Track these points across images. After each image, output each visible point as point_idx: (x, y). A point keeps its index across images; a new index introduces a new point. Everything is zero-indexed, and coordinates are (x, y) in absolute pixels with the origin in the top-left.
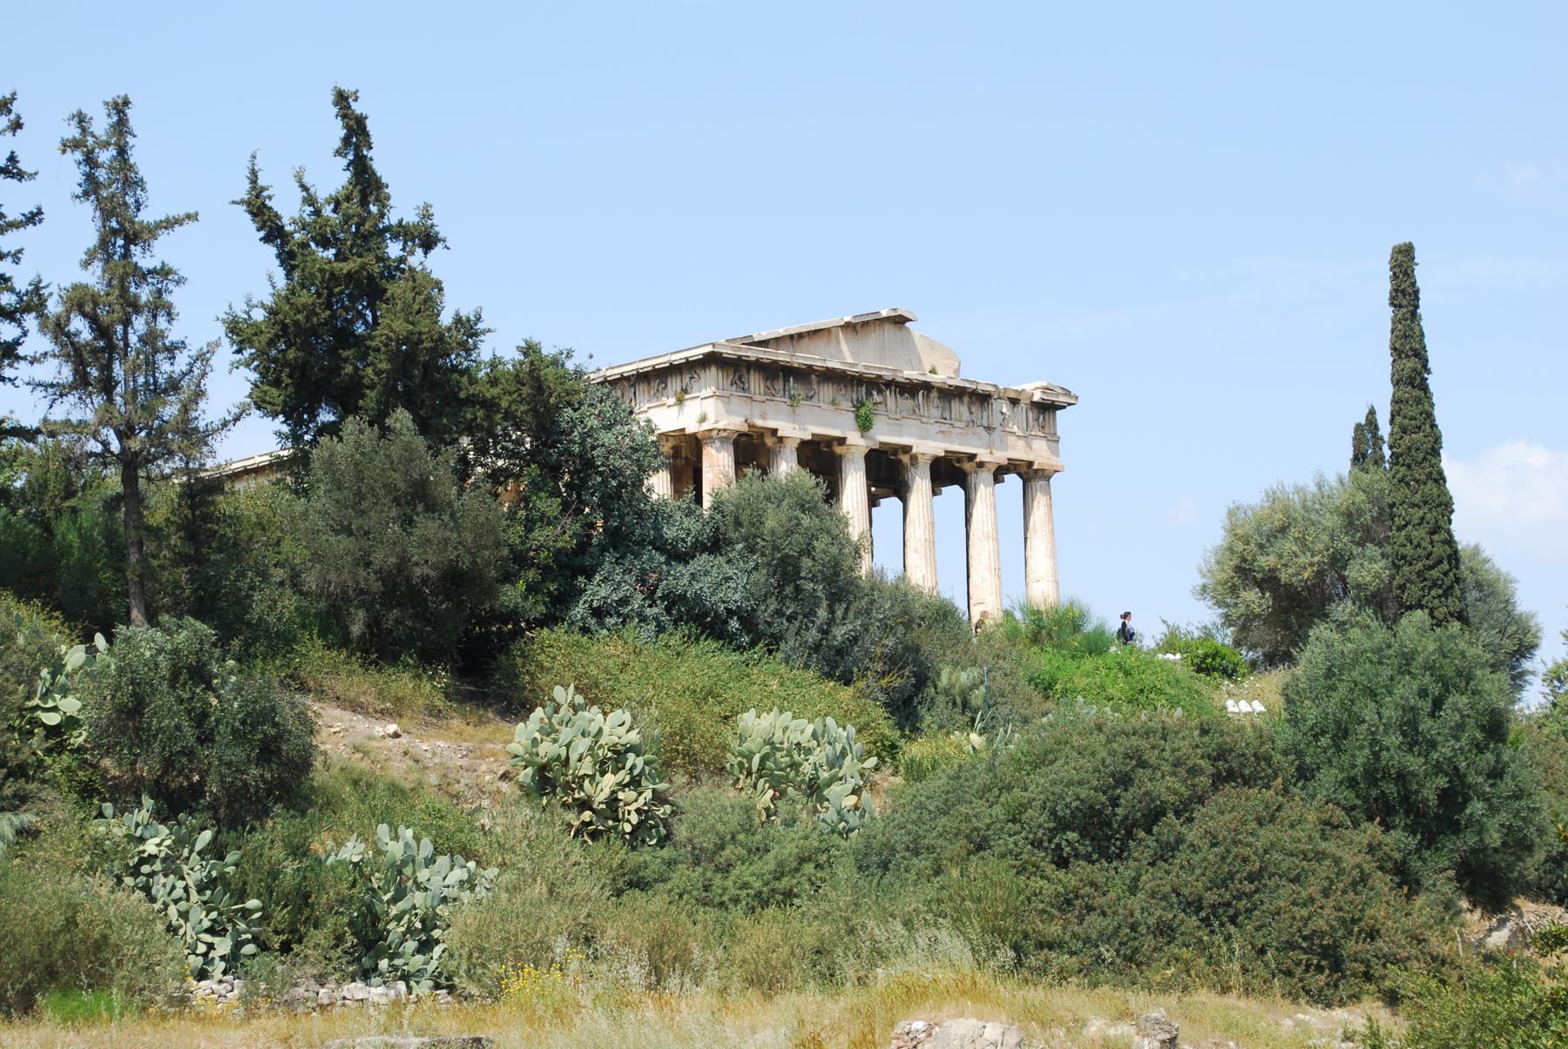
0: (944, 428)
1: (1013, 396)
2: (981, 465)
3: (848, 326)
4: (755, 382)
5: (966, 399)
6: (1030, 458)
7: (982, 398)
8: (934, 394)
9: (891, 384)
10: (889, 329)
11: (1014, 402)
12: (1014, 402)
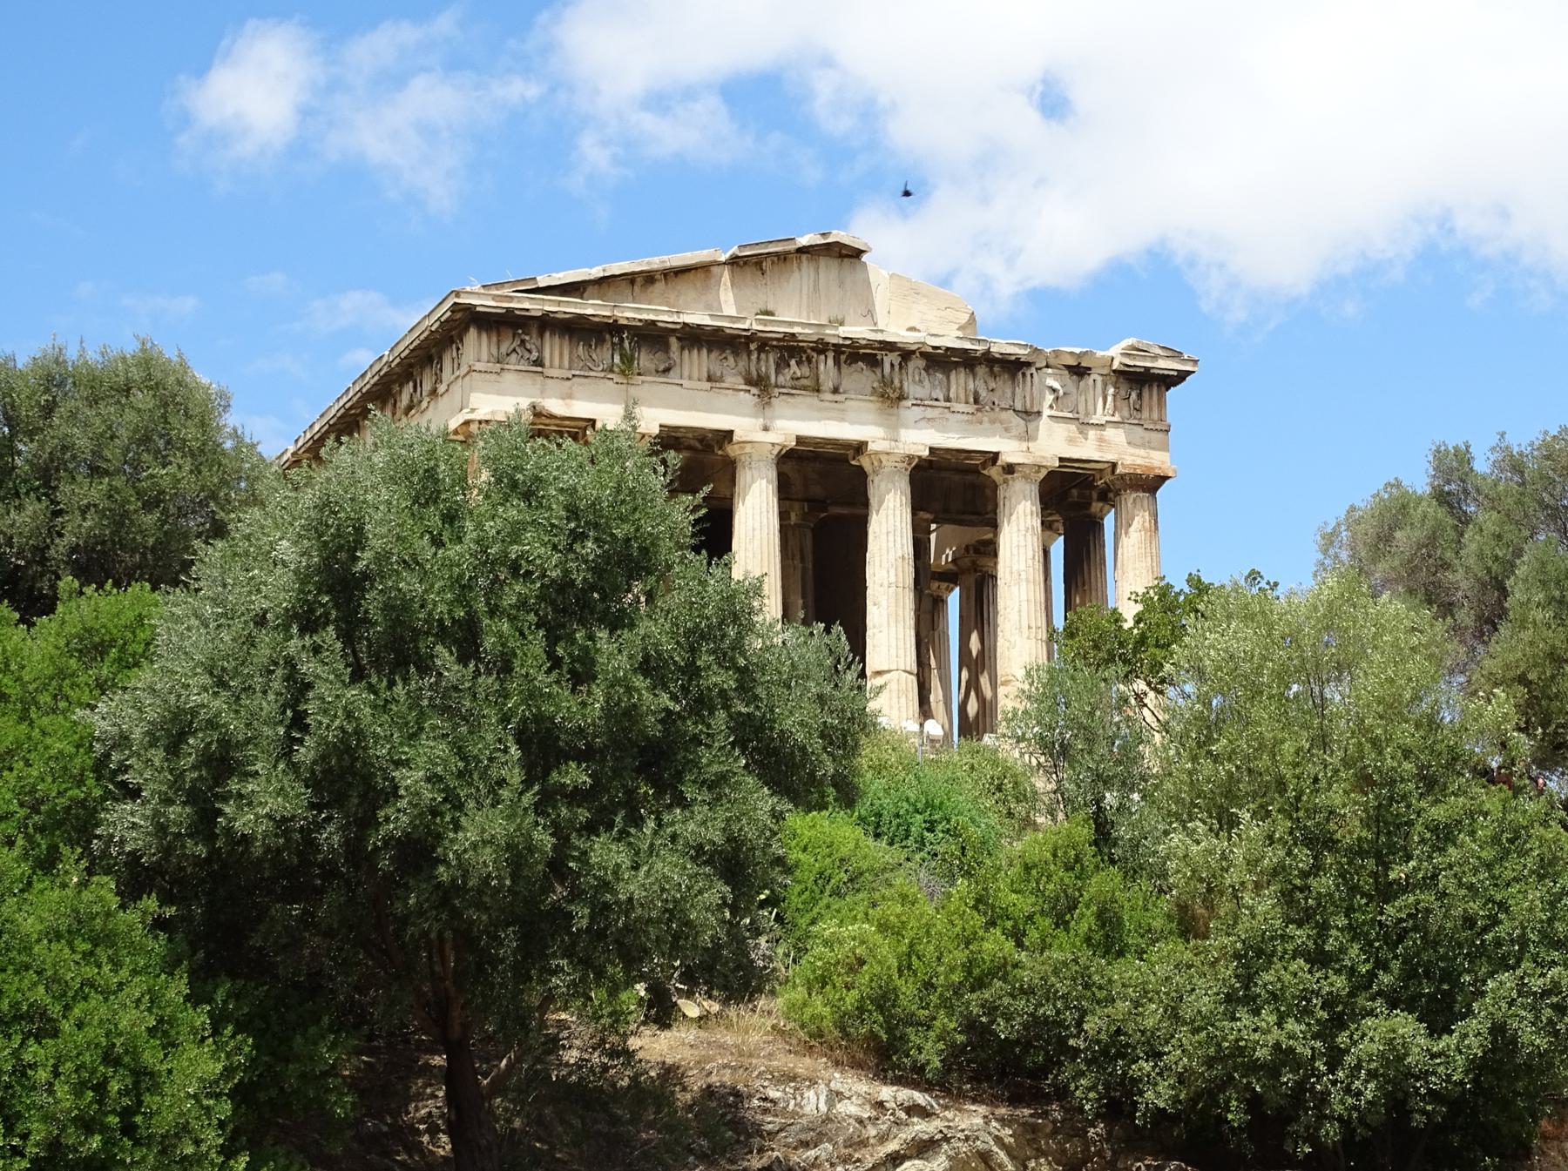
0: (930, 413)
1: (1073, 362)
2: (1010, 469)
3: (734, 262)
6: (1110, 457)
7: (1013, 367)
8: (917, 363)
9: (821, 347)
10: (829, 270)
11: (1079, 371)
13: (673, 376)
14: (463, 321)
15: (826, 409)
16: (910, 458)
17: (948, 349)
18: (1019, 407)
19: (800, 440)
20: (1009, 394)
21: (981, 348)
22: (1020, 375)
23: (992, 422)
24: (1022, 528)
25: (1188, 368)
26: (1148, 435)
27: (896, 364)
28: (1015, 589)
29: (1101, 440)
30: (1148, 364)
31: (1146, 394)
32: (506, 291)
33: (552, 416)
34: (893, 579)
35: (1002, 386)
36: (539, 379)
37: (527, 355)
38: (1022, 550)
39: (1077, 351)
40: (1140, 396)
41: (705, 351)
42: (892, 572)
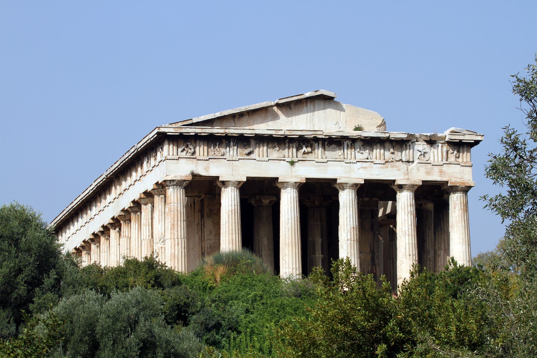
2: (401, 187)
3: (278, 105)
6: (445, 179)
9: (316, 140)
12: (431, 142)
13: (252, 156)
14: (161, 139)
15: (319, 166)
16: (356, 185)
17: (371, 137)
18: (404, 160)
19: (307, 179)
21: (387, 135)
23: (392, 167)
25: (479, 138)
27: (349, 144)
28: (403, 239)
29: (441, 172)
30: (461, 138)
32: (180, 124)
33: (200, 176)
34: (349, 237)
36: (195, 160)
37: (190, 151)
38: (407, 222)
39: (429, 134)
42: (349, 234)
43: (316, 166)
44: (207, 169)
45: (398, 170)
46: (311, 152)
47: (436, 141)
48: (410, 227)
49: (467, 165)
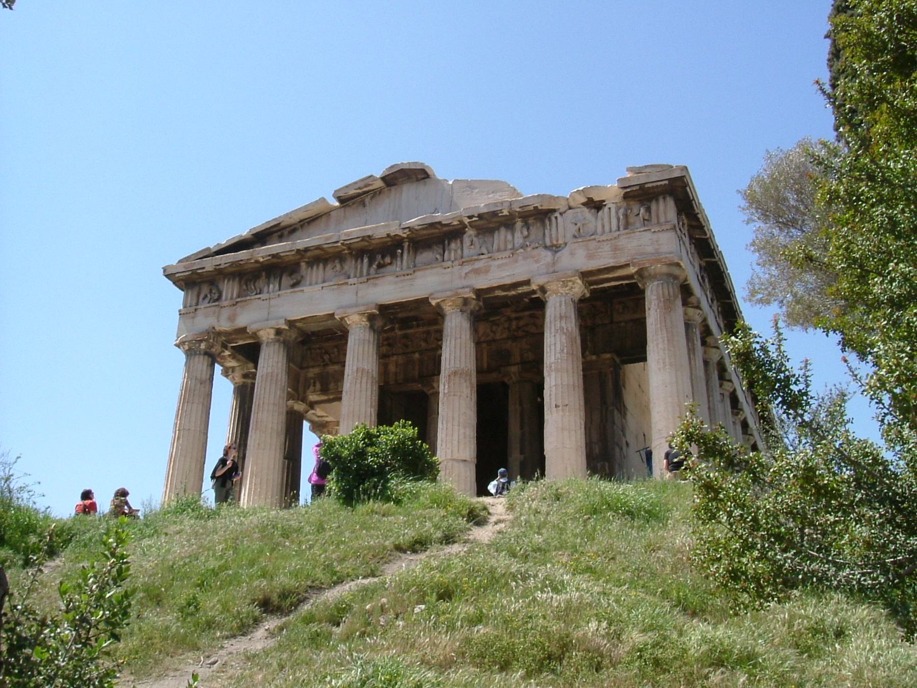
2: (543, 289)
4: (229, 289)
5: (519, 224)
7: (539, 215)
18: (548, 244)
20: (541, 234)
22: (547, 222)
23: (525, 258)
24: (553, 330)
26: (655, 236)
29: (615, 249)
31: (653, 206)
35: (535, 231)
38: (553, 347)
40: (648, 210)
41: (321, 265)
43: (396, 283)
44: (232, 318)
45: (537, 262)
46: (390, 264)
47: (604, 201)
48: (558, 355)
49: (664, 227)
